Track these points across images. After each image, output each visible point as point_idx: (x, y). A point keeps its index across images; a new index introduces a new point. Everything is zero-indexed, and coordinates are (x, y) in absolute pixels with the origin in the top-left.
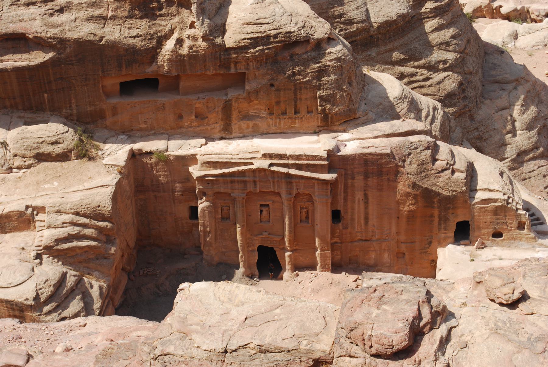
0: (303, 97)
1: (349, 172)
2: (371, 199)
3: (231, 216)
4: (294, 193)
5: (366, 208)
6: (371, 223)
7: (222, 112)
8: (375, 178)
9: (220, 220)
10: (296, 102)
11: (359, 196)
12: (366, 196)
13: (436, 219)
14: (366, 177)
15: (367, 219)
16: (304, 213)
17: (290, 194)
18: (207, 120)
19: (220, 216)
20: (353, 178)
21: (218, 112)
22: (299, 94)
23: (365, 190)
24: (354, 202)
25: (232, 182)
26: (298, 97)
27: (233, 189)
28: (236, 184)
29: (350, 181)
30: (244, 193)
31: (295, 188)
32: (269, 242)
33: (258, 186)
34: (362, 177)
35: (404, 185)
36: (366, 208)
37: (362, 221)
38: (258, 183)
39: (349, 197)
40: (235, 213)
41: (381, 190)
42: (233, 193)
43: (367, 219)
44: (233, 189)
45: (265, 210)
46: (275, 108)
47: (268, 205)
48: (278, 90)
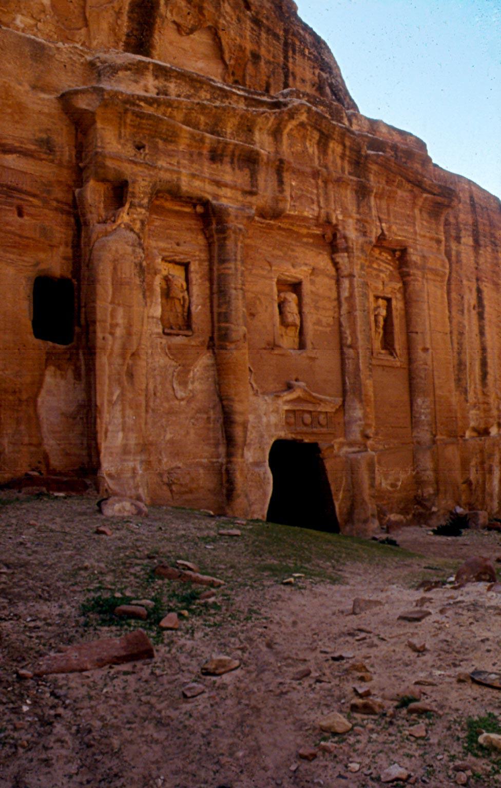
0: (298, 71)
1: (452, 220)
3: (196, 309)
4: (375, 233)
5: (482, 333)
6: (490, 378)
7: (129, 18)
8: (489, 249)
10: (286, 77)
12: (479, 291)
14: (477, 245)
15: (484, 364)
16: (381, 323)
17: (364, 234)
18: (83, 31)
20: (458, 239)
21: (119, 14)
22: (291, 60)
23: (478, 279)
24: (462, 311)
25: (215, 156)
26: (290, 66)
28: (228, 168)
29: (453, 245)
33: (287, 188)
34: (470, 241)
36: (482, 333)
38: (287, 176)
43: (484, 364)
45: (292, 297)
46: (250, 69)
47: (296, 287)
48: (256, 21)
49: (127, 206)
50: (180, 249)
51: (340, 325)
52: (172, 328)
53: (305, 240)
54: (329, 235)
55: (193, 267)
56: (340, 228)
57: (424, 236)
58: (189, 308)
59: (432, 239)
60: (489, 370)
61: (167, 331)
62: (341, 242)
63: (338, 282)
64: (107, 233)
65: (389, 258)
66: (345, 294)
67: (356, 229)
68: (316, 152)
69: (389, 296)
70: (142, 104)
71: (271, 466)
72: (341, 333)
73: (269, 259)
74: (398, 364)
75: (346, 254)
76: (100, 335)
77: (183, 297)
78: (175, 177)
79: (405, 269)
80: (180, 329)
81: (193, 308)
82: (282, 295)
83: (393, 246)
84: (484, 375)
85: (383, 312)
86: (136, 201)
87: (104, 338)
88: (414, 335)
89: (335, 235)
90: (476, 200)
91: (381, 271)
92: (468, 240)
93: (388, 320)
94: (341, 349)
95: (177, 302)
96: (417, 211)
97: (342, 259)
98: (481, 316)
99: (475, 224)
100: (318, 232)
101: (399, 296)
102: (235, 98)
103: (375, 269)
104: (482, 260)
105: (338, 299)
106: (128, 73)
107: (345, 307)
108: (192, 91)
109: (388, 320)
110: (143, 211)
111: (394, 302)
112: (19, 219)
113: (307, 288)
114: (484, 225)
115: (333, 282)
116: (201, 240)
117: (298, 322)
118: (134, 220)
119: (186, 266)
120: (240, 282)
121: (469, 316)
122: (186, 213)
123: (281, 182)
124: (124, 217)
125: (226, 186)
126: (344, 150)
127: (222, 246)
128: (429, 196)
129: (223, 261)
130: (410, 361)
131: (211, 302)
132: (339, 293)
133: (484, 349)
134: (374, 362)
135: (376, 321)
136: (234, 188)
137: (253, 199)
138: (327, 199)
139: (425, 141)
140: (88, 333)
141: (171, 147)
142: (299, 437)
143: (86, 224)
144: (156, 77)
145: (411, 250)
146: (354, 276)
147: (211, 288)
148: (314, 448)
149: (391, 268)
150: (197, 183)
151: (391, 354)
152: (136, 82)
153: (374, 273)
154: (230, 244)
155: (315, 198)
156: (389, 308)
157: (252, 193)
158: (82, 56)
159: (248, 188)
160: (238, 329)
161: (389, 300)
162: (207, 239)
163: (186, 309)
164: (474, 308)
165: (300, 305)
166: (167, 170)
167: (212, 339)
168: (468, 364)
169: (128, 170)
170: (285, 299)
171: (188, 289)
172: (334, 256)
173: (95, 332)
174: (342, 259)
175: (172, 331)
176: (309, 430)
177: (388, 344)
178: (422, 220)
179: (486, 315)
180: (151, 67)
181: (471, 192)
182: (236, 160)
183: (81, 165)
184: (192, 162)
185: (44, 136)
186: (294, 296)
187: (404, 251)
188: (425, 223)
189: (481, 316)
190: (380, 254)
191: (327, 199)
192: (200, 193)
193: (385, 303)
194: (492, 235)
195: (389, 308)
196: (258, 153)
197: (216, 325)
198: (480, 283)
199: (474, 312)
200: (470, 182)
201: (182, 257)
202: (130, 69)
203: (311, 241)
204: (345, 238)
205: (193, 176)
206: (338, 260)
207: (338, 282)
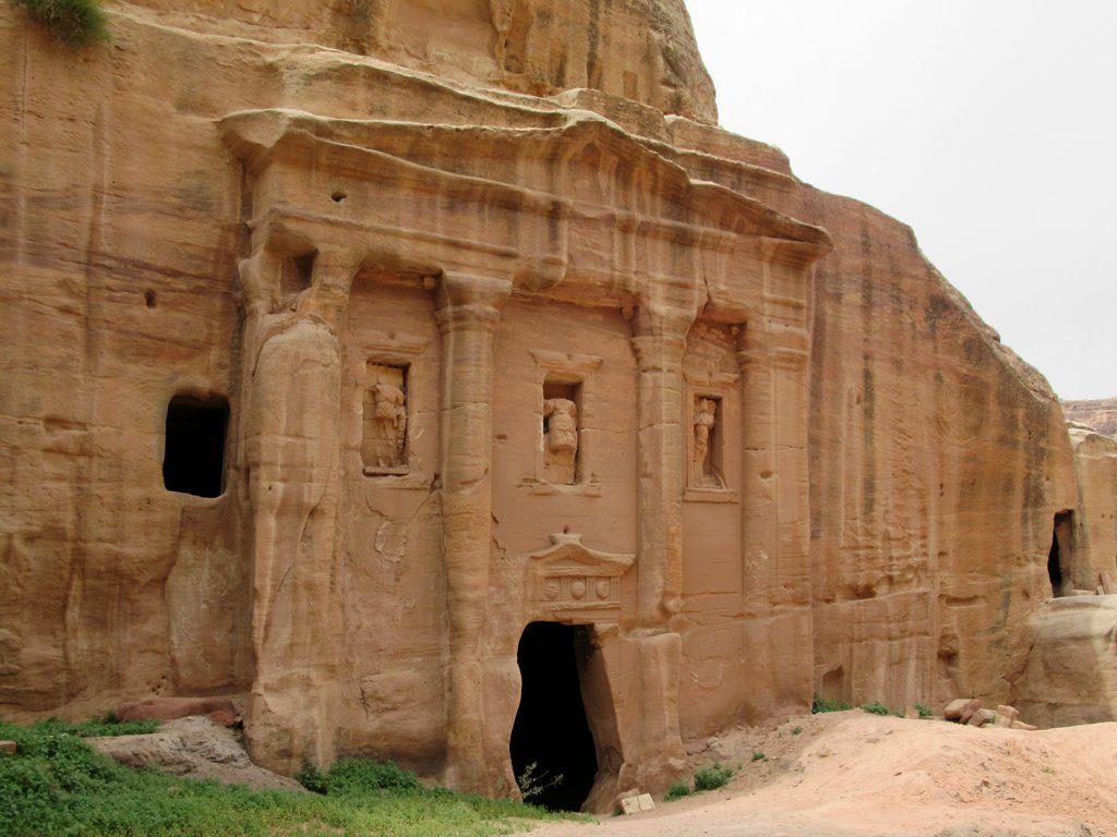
1: (829, 270)
2: (880, 396)
3: (415, 436)
9: (358, 462)
11: (852, 384)
13: (1018, 496)
15: (869, 486)
16: (705, 432)
19: (357, 439)
20: (838, 297)
27: (456, 245)
29: (828, 308)
30: (505, 273)
31: (698, 281)
32: (579, 586)
35: (951, 352)
37: (858, 494)
39: (827, 384)
40: (445, 408)
41: (897, 365)
42: (455, 265)
43: (869, 486)
44: (456, 245)
45: (564, 406)
47: (572, 391)
49: (315, 287)
50: (394, 343)
51: (638, 445)
52: (378, 465)
53: (591, 318)
54: (628, 309)
55: (413, 371)
56: (644, 299)
57: (775, 302)
58: (406, 432)
59: (786, 304)
60: (877, 495)
61: (370, 469)
62: (643, 320)
63: (638, 378)
64: (281, 329)
65: (722, 336)
66: (647, 395)
67: (668, 299)
68: (613, 183)
69: (719, 394)
70: (345, 133)
71: (519, 662)
72: (638, 456)
73: (531, 350)
74: (727, 498)
75: (651, 338)
76: (264, 484)
77: (398, 417)
78: (390, 239)
79: (744, 353)
80: (390, 465)
81: (411, 433)
82: (551, 402)
83: (729, 319)
84: (869, 505)
85: (708, 419)
86: (329, 280)
87: (270, 488)
88: (752, 453)
89: (636, 309)
90: (871, 231)
91: (707, 357)
92: (853, 297)
93: (714, 432)
94: (638, 482)
95: (388, 426)
96: (766, 266)
97: (644, 342)
98: (868, 414)
99: (867, 271)
100: (613, 305)
101: (734, 393)
102: (492, 111)
103: (700, 355)
104: (875, 326)
105: (638, 405)
106: (328, 82)
107: (646, 415)
108: (425, 104)
109: (714, 432)
110: (341, 293)
111: (726, 404)
112: (152, 311)
113: (590, 390)
114: (882, 271)
115: (631, 380)
116: (430, 325)
117: (575, 445)
118: (326, 306)
119: (404, 369)
120: (483, 391)
121: (850, 414)
122: (408, 288)
123: (554, 236)
124: (309, 298)
125: (469, 247)
126: (656, 182)
127: (460, 342)
128: (785, 241)
129: (458, 362)
130: (745, 490)
131: (440, 419)
132: (639, 395)
133: (870, 465)
134: (689, 496)
135: (696, 433)
136: (481, 250)
137: (511, 265)
138: (626, 259)
139: (786, 151)
140: (248, 480)
141: (388, 194)
142: (565, 616)
143: (253, 314)
144: (370, 87)
145: (751, 324)
146: (660, 370)
147: (441, 400)
148: (587, 630)
149: (724, 352)
150: (423, 248)
151: (718, 484)
152: (339, 97)
153: (698, 359)
154: (472, 337)
155: (606, 257)
156: (717, 415)
157: (507, 255)
158: (258, 55)
159: (503, 248)
160: (476, 461)
161: (717, 401)
162: (439, 326)
163: (401, 434)
164: (858, 402)
165: (577, 414)
166: (378, 231)
167: (437, 476)
168: (843, 490)
169: (318, 236)
170: (555, 409)
171: (405, 404)
172: (635, 339)
173: (257, 479)
174: (644, 342)
175: (378, 470)
176: (582, 604)
177: (713, 467)
178: (773, 277)
179: (877, 411)
180: (362, 73)
181: (865, 224)
182: (486, 208)
183: (249, 223)
184: (419, 214)
185: (194, 182)
186: (570, 403)
187: (743, 326)
188: (777, 282)
189: (868, 414)
190: (708, 331)
191: (626, 259)
192: (427, 262)
193: (714, 404)
194: (896, 286)
195: (717, 415)
196: (520, 195)
197: (446, 458)
198: (869, 362)
199: (858, 408)
200: (864, 208)
201: (398, 356)
202: (330, 78)
203: (601, 318)
204: (650, 314)
205: (417, 238)
206: (640, 345)
207: (638, 378)
